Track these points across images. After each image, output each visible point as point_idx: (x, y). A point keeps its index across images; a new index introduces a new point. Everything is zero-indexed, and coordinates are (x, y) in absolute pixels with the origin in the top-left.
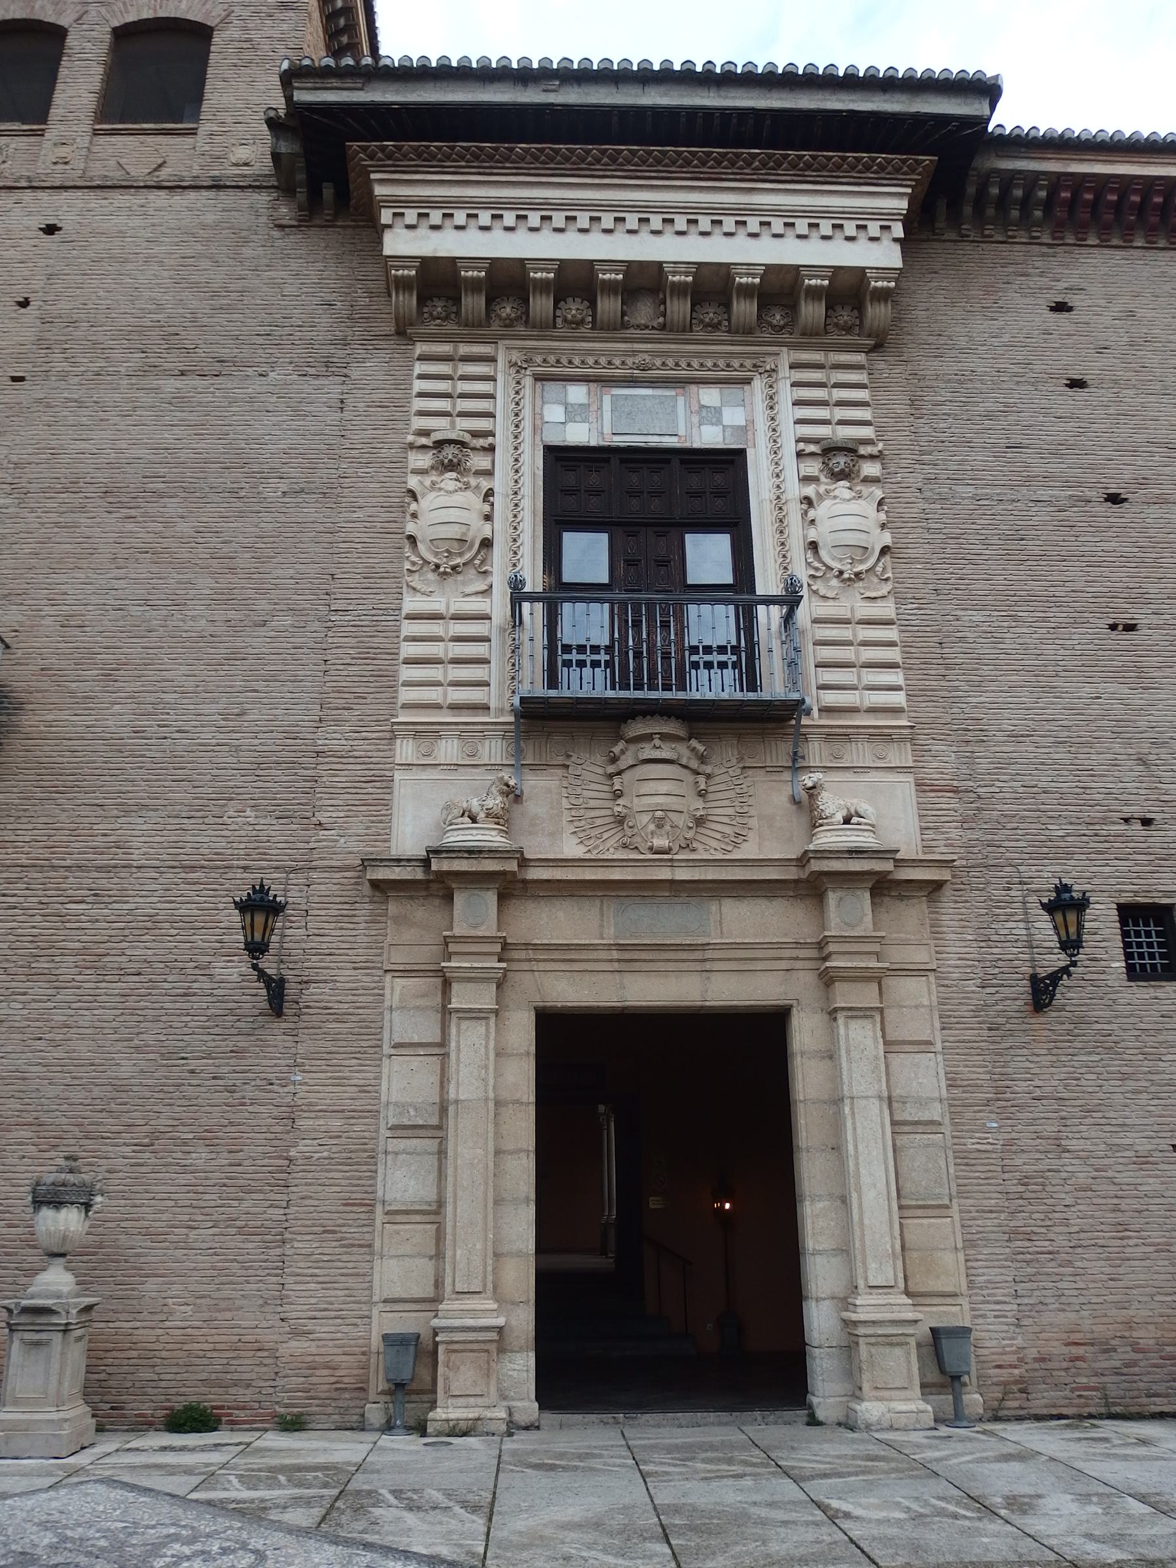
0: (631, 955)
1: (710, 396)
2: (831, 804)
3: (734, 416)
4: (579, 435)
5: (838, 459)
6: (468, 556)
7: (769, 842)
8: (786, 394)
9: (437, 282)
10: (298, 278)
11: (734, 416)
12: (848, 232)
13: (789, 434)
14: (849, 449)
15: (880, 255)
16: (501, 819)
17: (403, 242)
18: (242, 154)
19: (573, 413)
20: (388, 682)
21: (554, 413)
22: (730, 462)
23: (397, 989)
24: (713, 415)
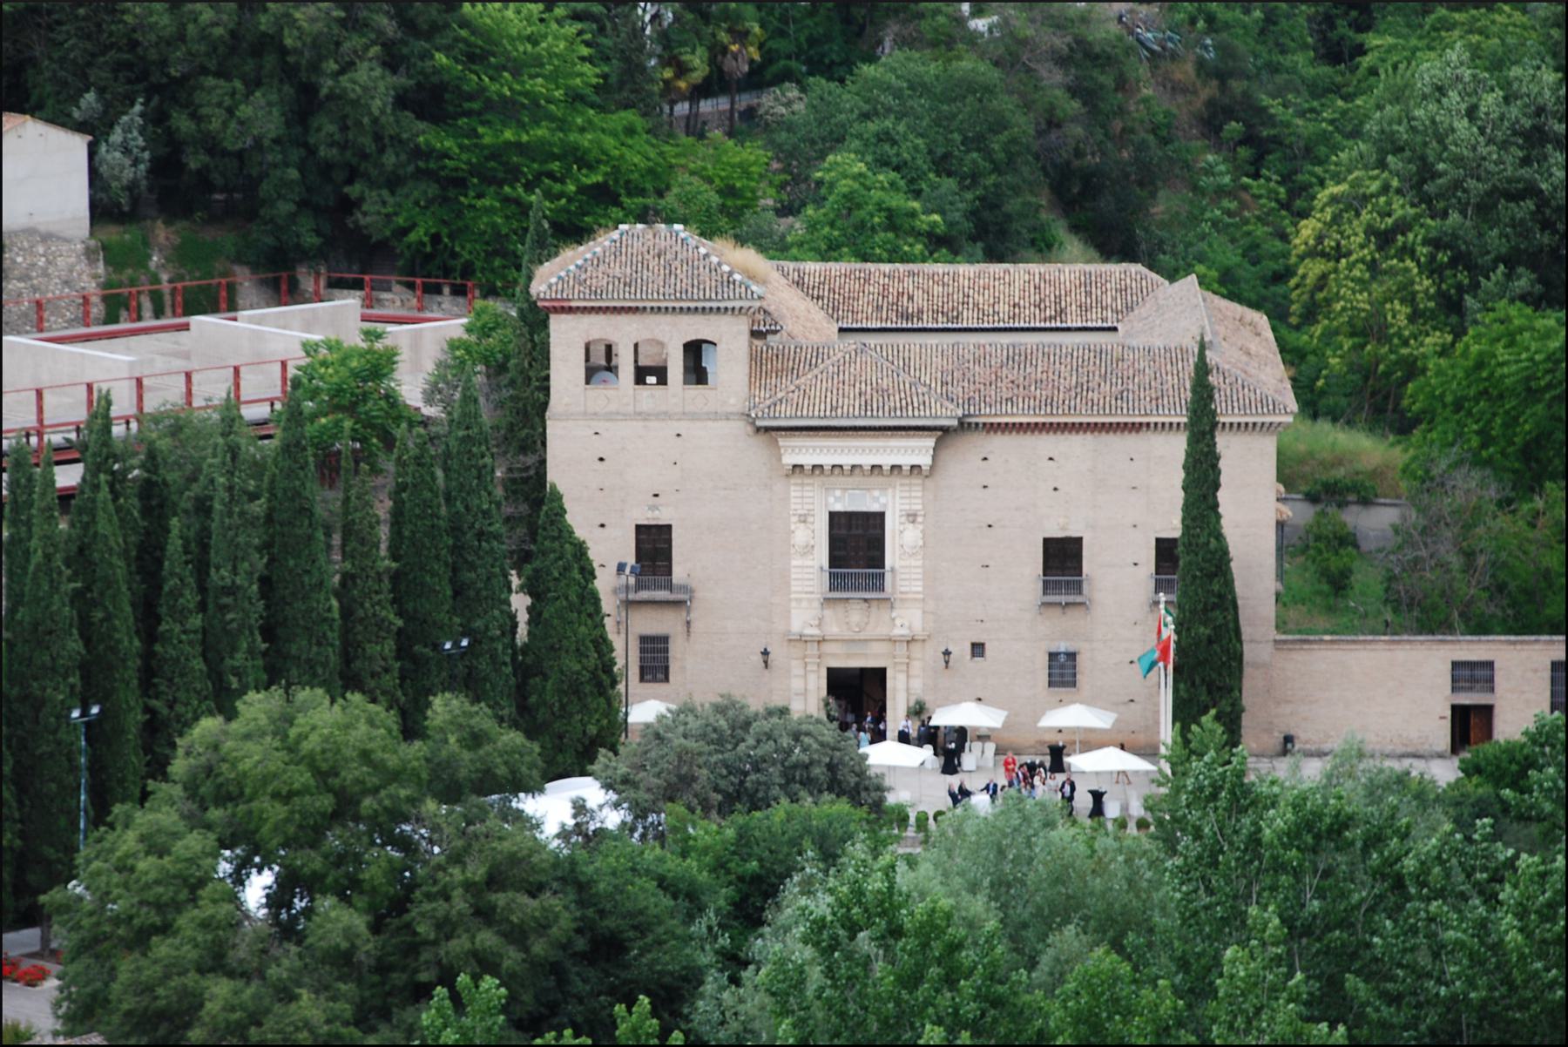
0: (848, 656)
1: (876, 493)
2: (898, 622)
3: (883, 500)
4: (839, 507)
5: (912, 517)
6: (809, 549)
7: (882, 631)
8: (898, 494)
9: (797, 468)
10: (754, 451)
11: (883, 500)
12: (918, 451)
13: (898, 507)
14: (915, 515)
15: (925, 460)
16: (819, 626)
17: (789, 459)
18: (732, 401)
19: (837, 499)
20: (788, 584)
21: (831, 500)
22: (880, 516)
23: (794, 663)
24: (876, 500)
